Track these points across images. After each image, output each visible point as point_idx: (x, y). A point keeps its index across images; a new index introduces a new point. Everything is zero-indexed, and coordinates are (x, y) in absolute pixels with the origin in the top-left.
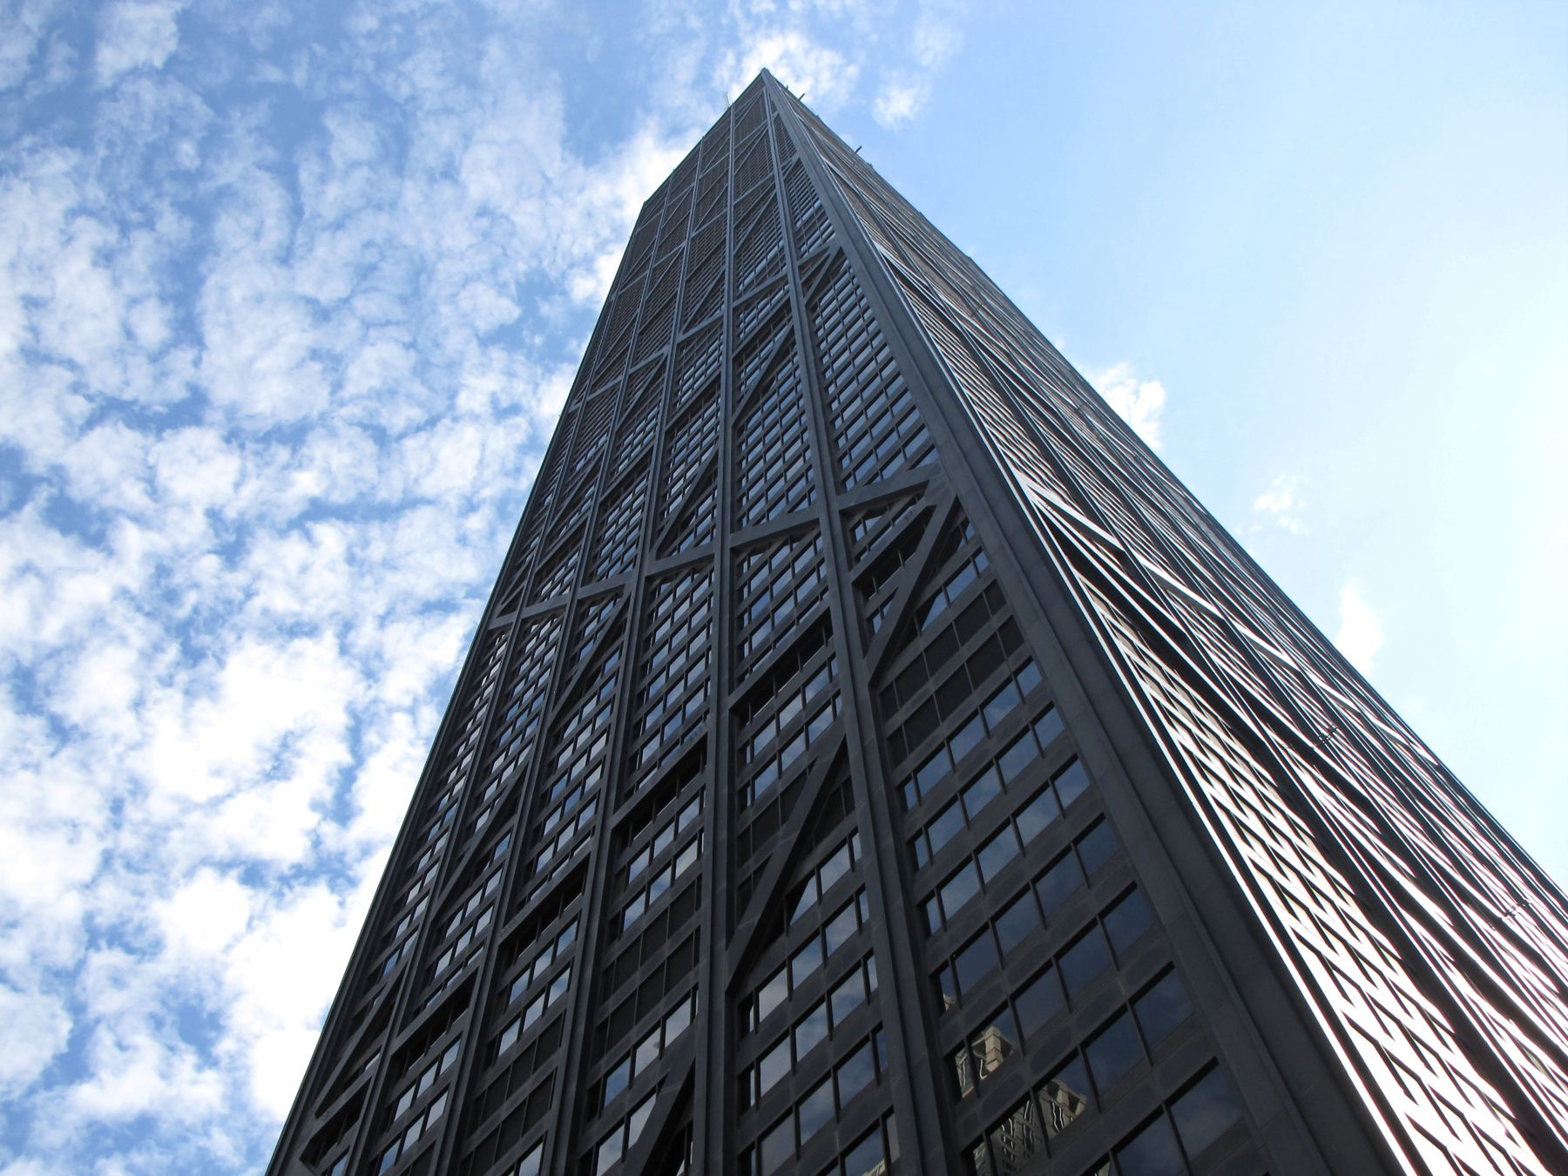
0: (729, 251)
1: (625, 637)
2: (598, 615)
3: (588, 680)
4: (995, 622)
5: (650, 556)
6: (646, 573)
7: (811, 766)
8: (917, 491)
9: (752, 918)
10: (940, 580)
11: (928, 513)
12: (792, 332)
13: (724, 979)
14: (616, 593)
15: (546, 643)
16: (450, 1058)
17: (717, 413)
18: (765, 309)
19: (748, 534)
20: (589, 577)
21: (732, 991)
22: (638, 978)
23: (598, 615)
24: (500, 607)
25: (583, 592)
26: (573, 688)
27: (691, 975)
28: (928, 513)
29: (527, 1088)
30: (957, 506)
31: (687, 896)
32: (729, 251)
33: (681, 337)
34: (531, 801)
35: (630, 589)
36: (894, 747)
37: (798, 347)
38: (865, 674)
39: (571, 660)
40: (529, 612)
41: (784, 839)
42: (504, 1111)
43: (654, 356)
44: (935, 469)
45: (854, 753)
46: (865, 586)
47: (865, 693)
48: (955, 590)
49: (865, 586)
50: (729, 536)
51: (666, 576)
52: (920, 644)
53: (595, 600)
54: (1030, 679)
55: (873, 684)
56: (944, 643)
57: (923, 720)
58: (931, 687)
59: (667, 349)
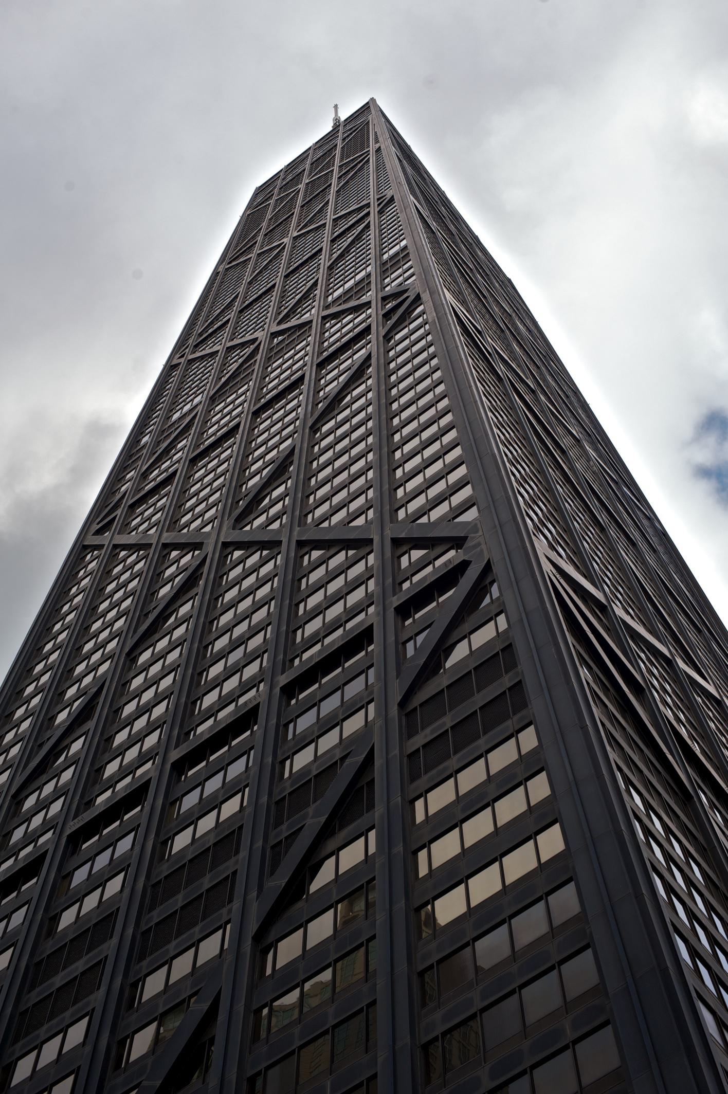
0: (324, 261)
3: (163, 616)
4: (507, 681)
6: (222, 539)
7: (343, 759)
8: (457, 542)
9: (280, 880)
11: (463, 566)
12: (369, 357)
13: (253, 926)
15: (131, 571)
16: (18, 918)
17: (297, 407)
18: (349, 325)
21: (258, 937)
22: (179, 900)
24: (95, 527)
25: (167, 537)
26: (148, 626)
27: (224, 911)
29: (80, 966)
30: (488, 568)
31: (227, 839)
32: (324, 261)
33: (275, 328)
34: (100, 711)
35: (209, 548)
39: (152, 594)
41: (314, 818)
42: (58, 980)
43: (248, 338)
44: (473, 526)
45: (378, 762)
46: (404, 611)
47: (394, 710)
49: (404, 611)
51: (238, 545)
52: (442, 681)
55: (402, 704)
58: (447, 721)
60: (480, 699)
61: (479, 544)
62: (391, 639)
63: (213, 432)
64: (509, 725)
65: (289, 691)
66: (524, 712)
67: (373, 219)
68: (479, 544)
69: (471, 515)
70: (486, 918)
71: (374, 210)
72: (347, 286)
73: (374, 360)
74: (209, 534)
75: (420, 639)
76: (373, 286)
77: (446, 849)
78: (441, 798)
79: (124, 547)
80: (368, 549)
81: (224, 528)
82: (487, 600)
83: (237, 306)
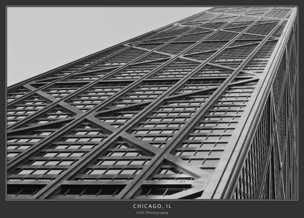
0: (226, 46)
1: (58, 130)
2: (59, 115)
5: (95, 113)
6: (86, 117)
14: (72, 114)
17: (166, 91)
19: (130, 137)
20: (69, 101)
23: (59, 115)
24: (34, 82)
25: (62, 103)
32: (226, 46)
35: (76, 117)
40: (40, 93)
53: (63, 109)
61: (204, 183)
63: (119, 78)
67: (261, 44)
71: (265, 40)
72: (228, 60)
73: (215, 93)
76: (239, 66)
79: (40, 97)
81: (91, 114)
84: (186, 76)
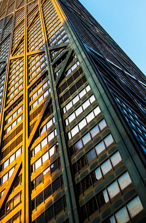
4: (81, 76)
5: (11, 56)
8: (65, 47)
10: (70, 66)
11: (67, 52)
12: (39, 11)
14: (5, 62)
19: (31, 53)
28: (67, 52)
33: (16, 10)
36: (60, 101)
37: (40, 15)
38: (55, 85)
43: (10, 14)
45: (53, 101)
46: (54, 66)
47: (55, 89)
48: (73, 68)
50: (27, 53)
51: (15, 60)
54: (88, 89)
56: (70, 80)
57: (67, 95)
59: (13, 13)
60: (75, 82)
61: (70, 47)
62: (52, 72)
63: (5, 36)
64: (83, 86)
65: (29, 91)
66: (86, 82)
68: (70, 47)
69: (68, 41)
70: (84, 132)
74: (7, 59)
75: (59, 71)
77: (72, 118)
78: (69, 106)
80: (44, 54)
82: (74, 59)
83: (7, 8)
84: (25, 15)
